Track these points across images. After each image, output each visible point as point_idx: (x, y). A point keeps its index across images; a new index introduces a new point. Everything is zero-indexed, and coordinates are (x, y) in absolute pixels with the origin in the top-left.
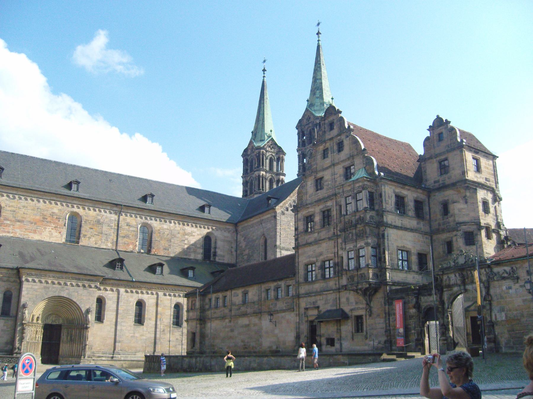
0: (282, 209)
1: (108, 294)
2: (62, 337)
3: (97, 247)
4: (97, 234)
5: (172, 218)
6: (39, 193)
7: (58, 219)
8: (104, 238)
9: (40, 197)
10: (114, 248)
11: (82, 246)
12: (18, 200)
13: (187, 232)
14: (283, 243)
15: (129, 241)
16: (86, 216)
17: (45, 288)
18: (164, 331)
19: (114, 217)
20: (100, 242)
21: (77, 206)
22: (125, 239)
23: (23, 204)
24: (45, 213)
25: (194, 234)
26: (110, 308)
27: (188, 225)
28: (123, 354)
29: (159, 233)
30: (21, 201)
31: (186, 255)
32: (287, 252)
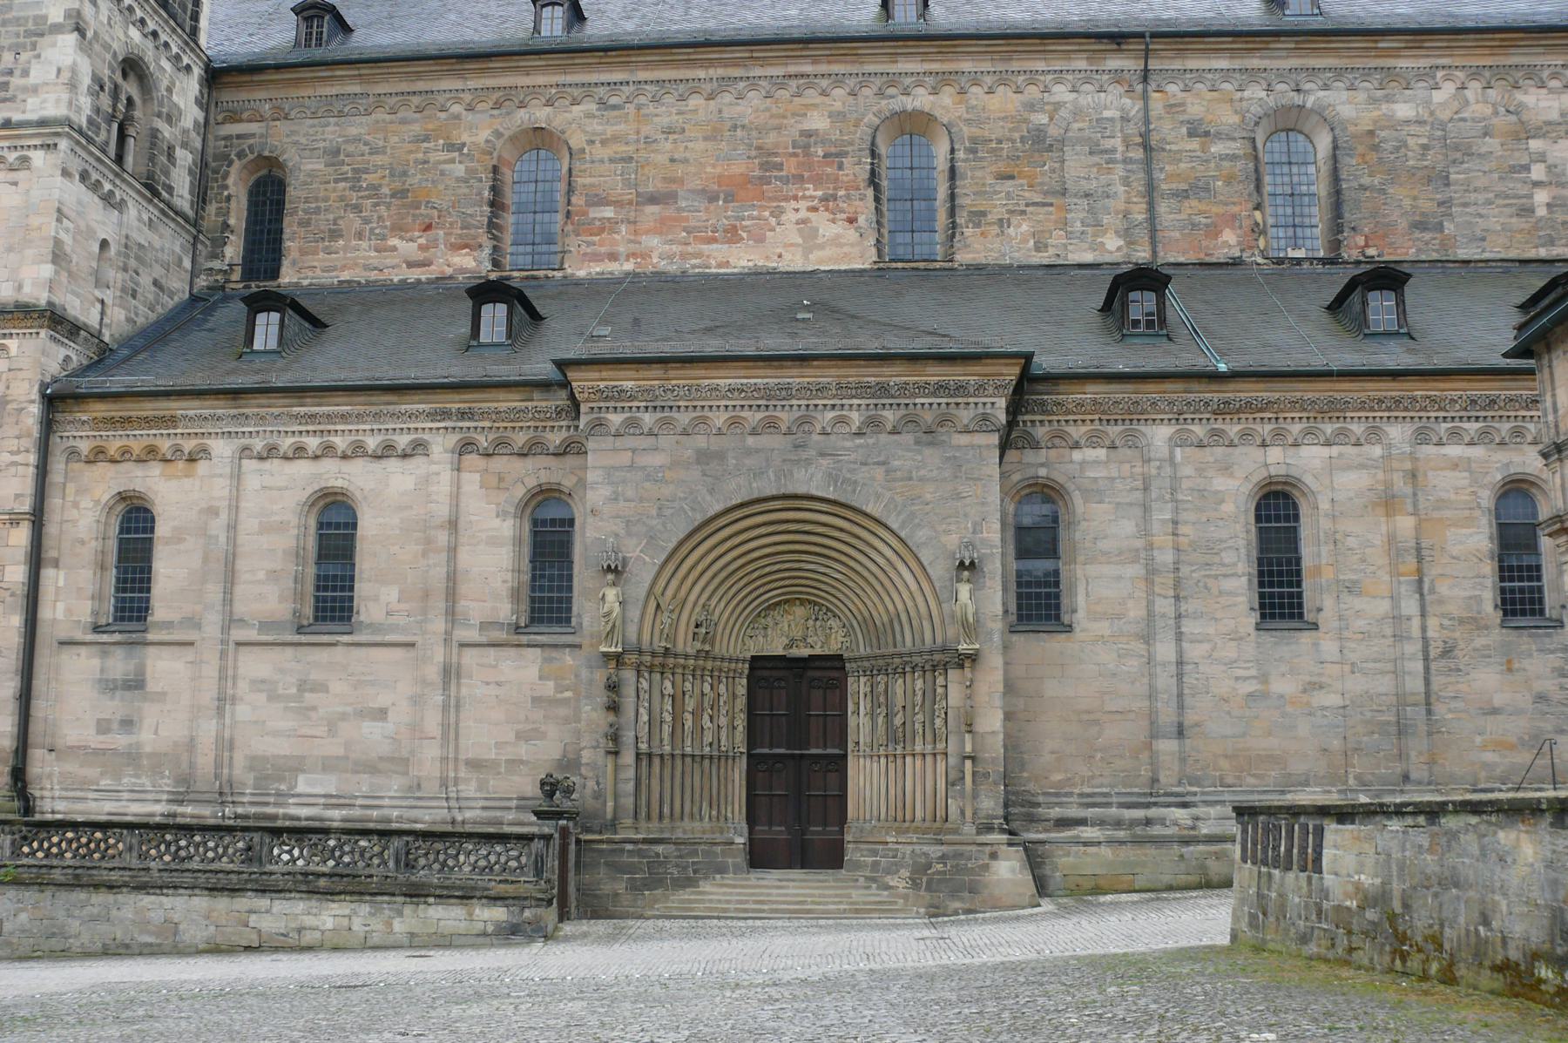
1: (1083, 463)
2: (852, 721)
3: (1045, 262)
7: (835, 156)
8: (1077, 217)
10: (1142, 255)
11: (968, 267)
15: (1219, 209)
16: (968, 122)
17: (703, 457)
18: (1447, 652)
19: (1115, 103)
20: (1057, 238)
23: (665, 121)
24: (771, 139)
26: (1103, 545)
28: (1205, 802)
29: (1375, 148)
30: (651, 109)
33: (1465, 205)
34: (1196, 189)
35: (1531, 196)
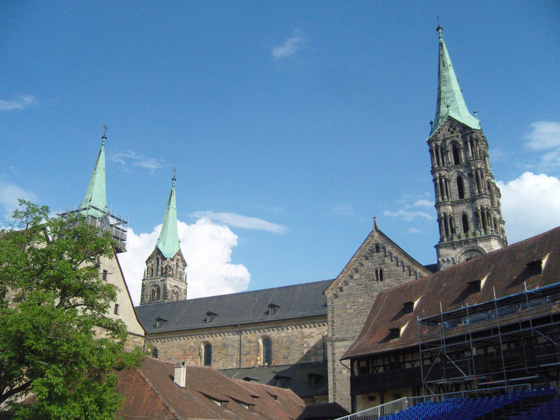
0: (334, 292)
3: (224, 369)
4: (224, 357)
5: (288, 324)
6: (179, 332)
9: (180, 335)
12: (167, 342)
13: (305, 334)
14: (338, 332)
16: (214, 342)
19: (237, 337)
21: (207, 336)
22: (248, 357)
25: (313, 335)
27: (306, 327)
29: (278, 342)
30: (169, 342)
31: (306, 359)
32: (342, 342)
33: (292, 353)
34: (248, 353)
35: (304, 350)
